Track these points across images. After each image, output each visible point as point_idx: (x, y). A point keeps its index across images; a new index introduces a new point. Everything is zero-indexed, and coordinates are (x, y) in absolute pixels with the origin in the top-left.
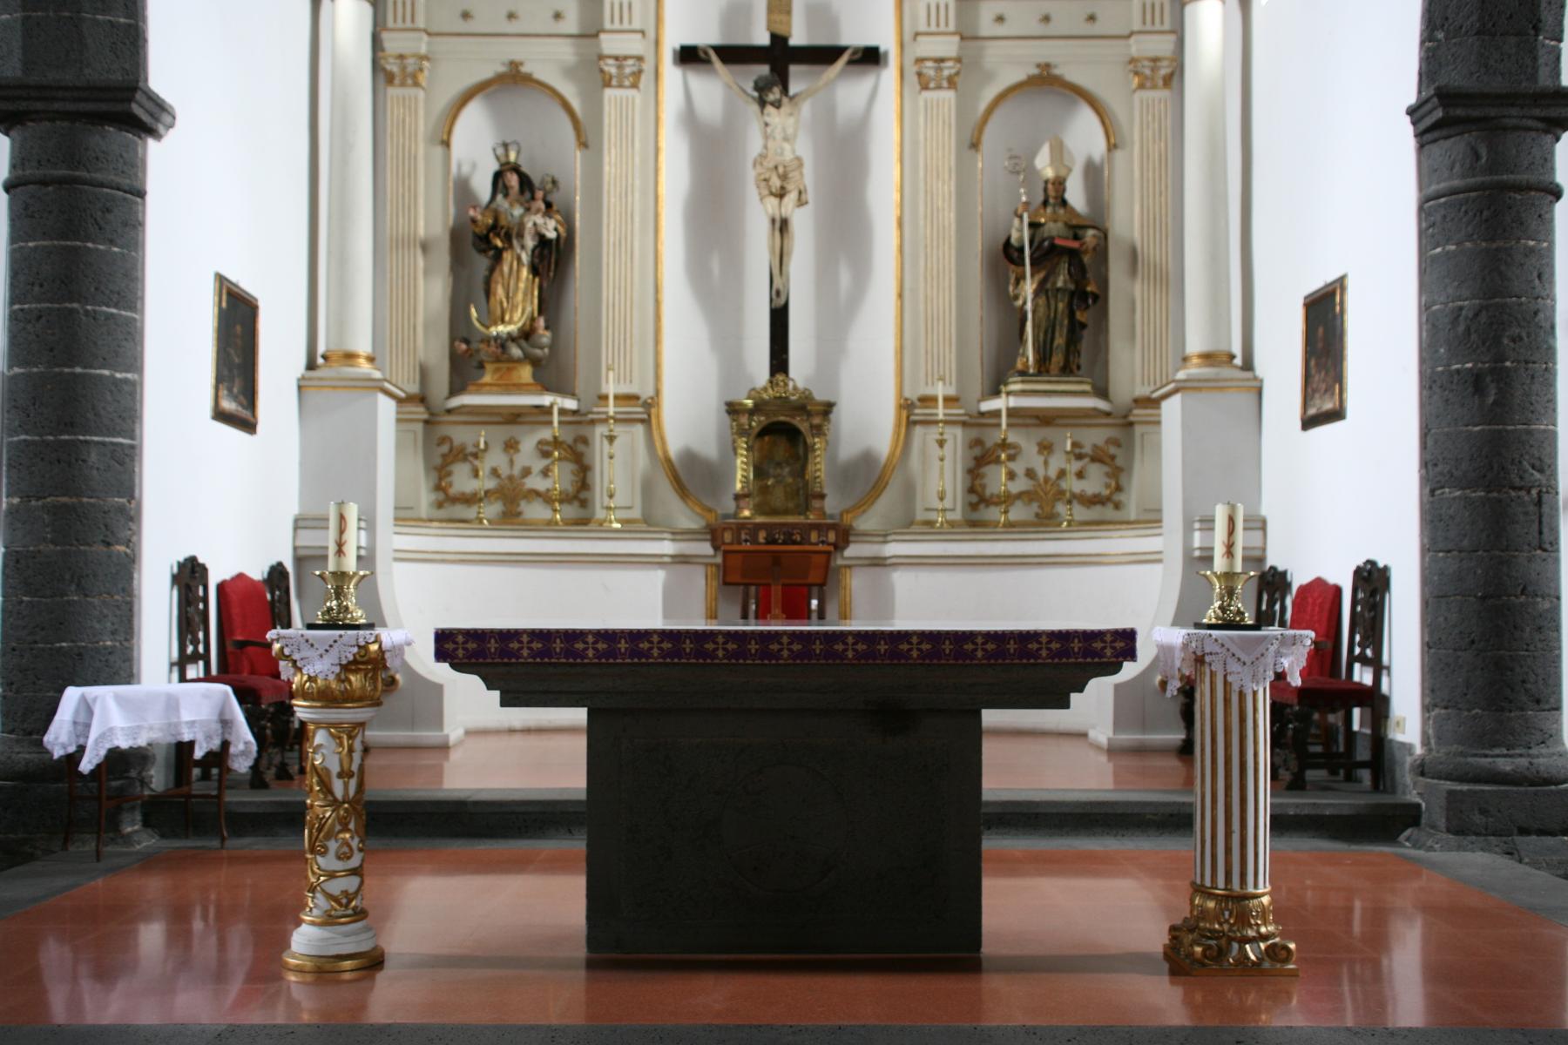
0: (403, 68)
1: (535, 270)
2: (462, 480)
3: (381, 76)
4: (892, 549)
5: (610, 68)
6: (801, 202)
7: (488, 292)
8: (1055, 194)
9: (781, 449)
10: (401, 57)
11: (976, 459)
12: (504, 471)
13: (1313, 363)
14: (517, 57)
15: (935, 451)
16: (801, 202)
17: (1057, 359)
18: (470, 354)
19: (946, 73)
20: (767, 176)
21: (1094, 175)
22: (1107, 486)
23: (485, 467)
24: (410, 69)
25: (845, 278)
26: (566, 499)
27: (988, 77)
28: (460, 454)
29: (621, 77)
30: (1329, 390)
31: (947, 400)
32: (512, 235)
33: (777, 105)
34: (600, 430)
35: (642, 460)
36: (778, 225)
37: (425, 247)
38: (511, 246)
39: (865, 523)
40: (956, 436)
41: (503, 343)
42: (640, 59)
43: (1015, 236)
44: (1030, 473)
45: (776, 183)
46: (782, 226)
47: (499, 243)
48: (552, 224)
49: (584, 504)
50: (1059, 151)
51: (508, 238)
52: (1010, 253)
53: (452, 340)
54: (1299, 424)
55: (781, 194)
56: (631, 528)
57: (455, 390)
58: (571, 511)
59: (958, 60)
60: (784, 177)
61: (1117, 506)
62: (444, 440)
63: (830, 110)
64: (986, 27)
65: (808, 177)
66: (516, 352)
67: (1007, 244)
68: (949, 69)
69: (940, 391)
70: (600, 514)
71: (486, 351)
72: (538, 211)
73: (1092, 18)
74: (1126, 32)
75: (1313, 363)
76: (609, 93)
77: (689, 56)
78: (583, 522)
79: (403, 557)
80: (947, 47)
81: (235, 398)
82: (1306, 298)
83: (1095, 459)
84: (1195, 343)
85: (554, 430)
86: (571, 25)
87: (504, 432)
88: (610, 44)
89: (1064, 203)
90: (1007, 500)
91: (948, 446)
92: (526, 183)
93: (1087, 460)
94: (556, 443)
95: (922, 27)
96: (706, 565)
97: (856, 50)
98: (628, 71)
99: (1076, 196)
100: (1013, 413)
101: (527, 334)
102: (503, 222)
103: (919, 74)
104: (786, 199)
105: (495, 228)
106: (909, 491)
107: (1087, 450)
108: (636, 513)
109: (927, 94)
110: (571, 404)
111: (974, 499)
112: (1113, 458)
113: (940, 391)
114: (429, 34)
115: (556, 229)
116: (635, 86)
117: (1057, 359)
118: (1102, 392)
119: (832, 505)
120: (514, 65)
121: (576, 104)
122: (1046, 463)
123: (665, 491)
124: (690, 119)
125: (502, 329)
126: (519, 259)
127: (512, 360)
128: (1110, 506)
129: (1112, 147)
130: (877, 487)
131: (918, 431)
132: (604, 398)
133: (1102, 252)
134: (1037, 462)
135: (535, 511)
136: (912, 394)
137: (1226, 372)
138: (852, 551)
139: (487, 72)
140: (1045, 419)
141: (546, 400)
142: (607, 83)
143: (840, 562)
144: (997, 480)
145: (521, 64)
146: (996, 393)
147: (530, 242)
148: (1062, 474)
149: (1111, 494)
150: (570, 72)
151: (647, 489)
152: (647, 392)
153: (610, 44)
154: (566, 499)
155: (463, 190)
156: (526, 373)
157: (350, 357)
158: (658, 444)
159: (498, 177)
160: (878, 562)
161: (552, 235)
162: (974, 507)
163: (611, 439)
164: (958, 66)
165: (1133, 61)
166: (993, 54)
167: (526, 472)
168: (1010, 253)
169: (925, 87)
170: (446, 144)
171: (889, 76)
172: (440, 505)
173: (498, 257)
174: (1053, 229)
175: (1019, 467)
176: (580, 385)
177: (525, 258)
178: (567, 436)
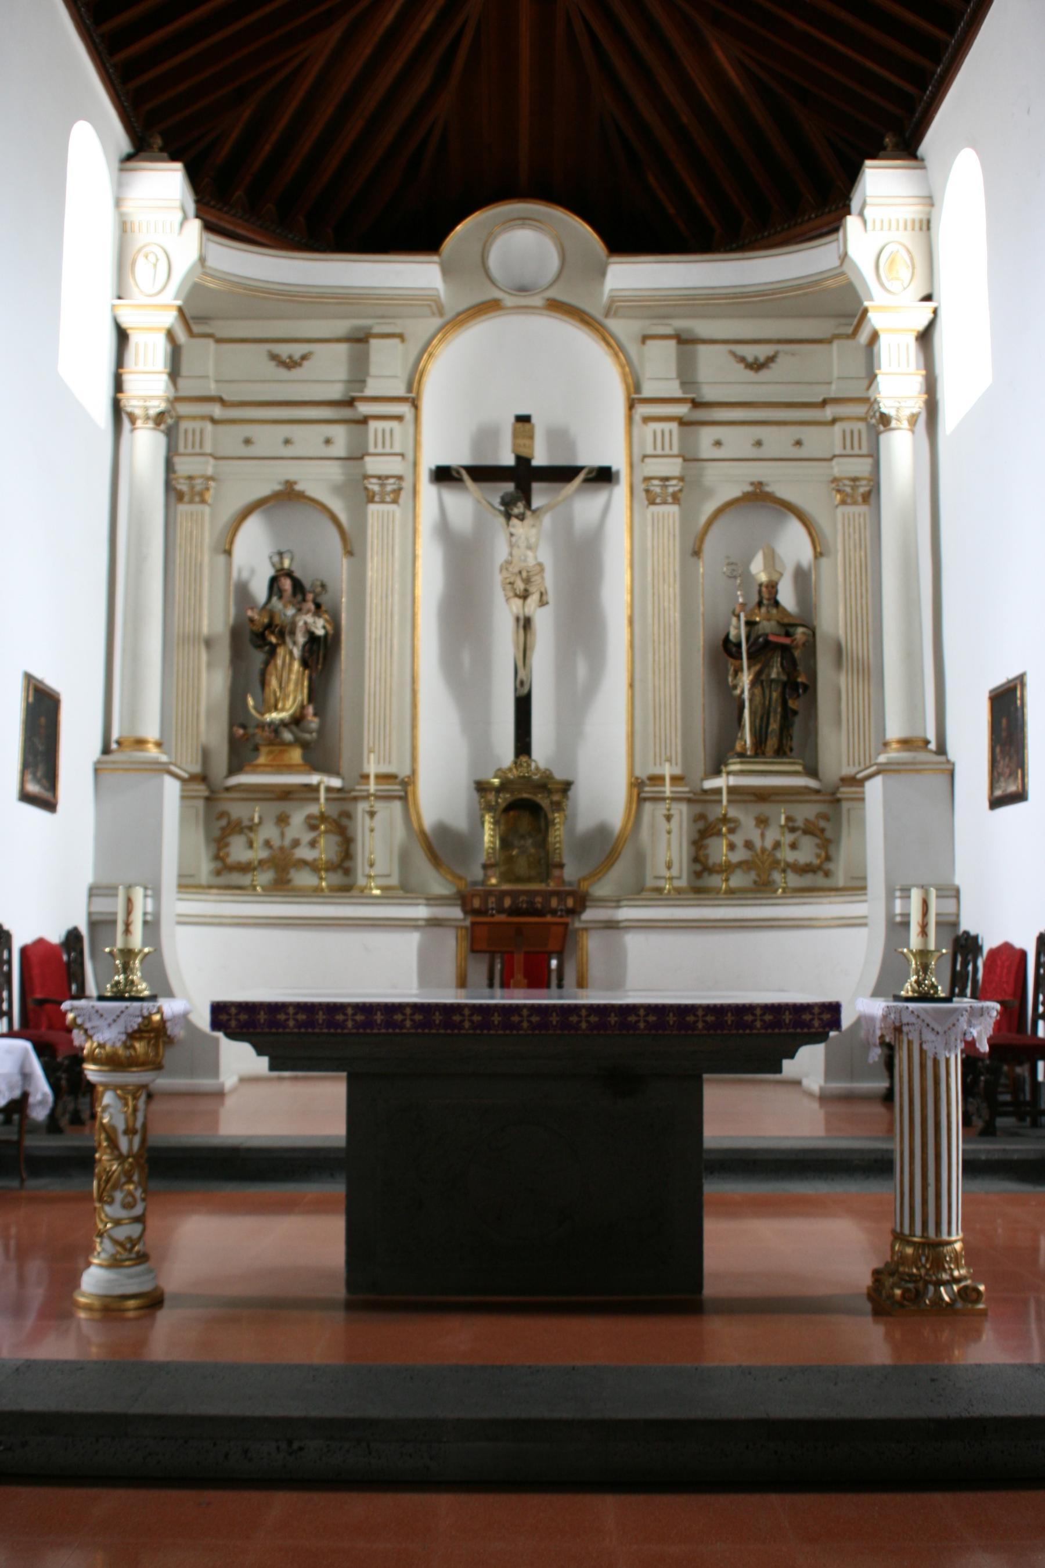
0: (192, 487)
1: (305, 663)
2: (239, 851)
3: (173, 495)
4: (625, 913)
5: (374, 486)
6: (543, 603)
7: (263, 683)
8: (768, 596)
9: (525, 822)
10: (190, 478)
12: (276, 842)
13: (998, 750)
14: (292, 477)
15: (663, 824)
16: (543, 603)
17: (772, 743)
18: (247, 738)
19: (671, 490)
20: (512, 580)
21: (802, 578)
22: (818, 856)
23: (260, 838)
24: (198, 488)
25: (582, 670)
26: (331, 867)
27: (708, 493)
28: (236, 827)
29: (383, 494)
30: (1012, 774)
31: (676, 779)
32: (284, 632)
33: (521, 517)
34: (362, 807)
35: (400, 833)
36: (522, 623)
37: (209, 643)
38: (284, 642)
39: (601, 889)
40: (682, 812)
41: (276, 728)
42: (400, 478)
43: (733, 632)
44: (749, 845)
45: (520, 586)
46: (526, 624)
47: (273, 639)
48: (320, 622)
49: (348, 872)
50: (772, 560)
51: (281, 635)
52: (729, 648)
53: (232, 724)
54: (986, 804)
55: (525, 596)
56: (389, 895)
57: (233, 771)
58: (336, 878)
59: (681, 479)
60: (527, 581)
61: (827, 874)
62: (223, 814)
63: (567, 525)
64: (706, 450)
65: (549, 581)
66: (288, 736)
67: (727, 640)
68: (673, 486)
69: (668, 770)
70: (361, 881)
71: (261, 736)
72: (308, 612)
73: (799, 443)
74: (828, 456)
75: (998, 750)
76: (372, 508)
77: (443, 475)
79: (185, 921)
80: (672, 467)
81: (38, 781)
82: (991, 692)
83: (806, 832)
84: (894, 731)
85: (321, 805)
86: (339, 448)
87: (277, 807)
88: (374, 465)
89: (776, 604)
90: (728, 869)
91: (675, 821)
92: (298, 587)
93: (799, 833)
94: (323, 817)
95: (650, 451)
96: (457, 927)
97: (592, 470)
98: (389, 488)
99: (787, 597)
100: (732, 790)
101: (297, 721)
102: (277, 621)
103: (647, 491)
104: (529, 601)
105: (270, 626)
106: (640, 860)
107: (800, 823)
108: (394, 881)
109: (653, 508)
110: (336, 782)
111: (698, 867)
112: (823, 830)
113: (668, 770)
114: (216, 458)
115: (324, 627)
116: (395, 501)
117: (772, 743)
118: (812, 771)
119: (570, 873)
120: (290, 484)
121: (343, 517)
122: (763, 835)
123: (421, 860)
124: (444, 530)
125: (275, 716)
126: (291, 653)
127: (284, 744)
128: (820, 874)
129: (818, 555)
130: (611, 857)
131: (648, 806)
132: (366, 777)
133: (810, 647)
134: (755, 835)
135: (304, 878)
136: (641, 773)
137: (922, 756)
138: (589, 915)
139: (264, 490)
140: (761, 796)
142: (371, 499)
143: (577, 925)
144: (719, 850)
145: (295, 483)
146: (717, 772)
147: (301, 639)
148: (777, 845)
149: (822, 863)
150: (338, 490)
151: (404, 859)
152: (404, 772)
153: (374, 465)
154: (331, 867)
155: (242, 593)
156: (296, 755)
157: (140, 743)
158: (414, 818)
159: (274, 581)
160: (612, 925)
161: (320, 632)
162: (698, 875)
163: (372, 814)
164: (681, 484)
165: (835, 480)
166: (712, 474)
167: (296, 843)
168: (729, 648)
169: (652, 502)
170: (229, 553)
171: (620, 492)
172: (218, 873)
173: (272, 652)
174: (767, 627)
175: (738, 839)
176: (345, 765)
177: (297, 652)
178: (333, 811)
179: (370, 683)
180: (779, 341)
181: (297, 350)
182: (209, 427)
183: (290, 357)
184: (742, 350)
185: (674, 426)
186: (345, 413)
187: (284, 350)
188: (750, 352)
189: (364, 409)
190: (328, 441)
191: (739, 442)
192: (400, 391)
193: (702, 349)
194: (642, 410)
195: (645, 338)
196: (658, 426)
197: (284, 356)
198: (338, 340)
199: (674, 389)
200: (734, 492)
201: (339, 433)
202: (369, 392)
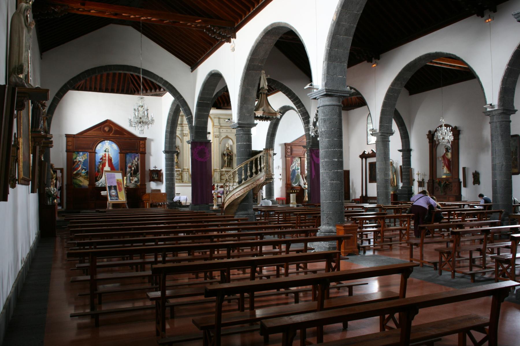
27: (221, 136)
34: (185, 173)
43: (224, 153)
64: (221, 131)
67: (223, 154)
78: (182, 182)
80: (218, 134)
99: (230, 149)
100: (225, 171)
121: (180, 138)
129: (233, 144)
133: (233, 155)
141: (179, 169)
142: (184, 136)
144: (223, 177)
150: (180, 134)
162: (220, 180)
166: (222, 134)
174: (228, 152)
176: (181, 168)
179: (185, 158)
189: (183, 125)
191: (225, 130)
193: (221, 119)
194: (214, 127)
200: (224, 136)
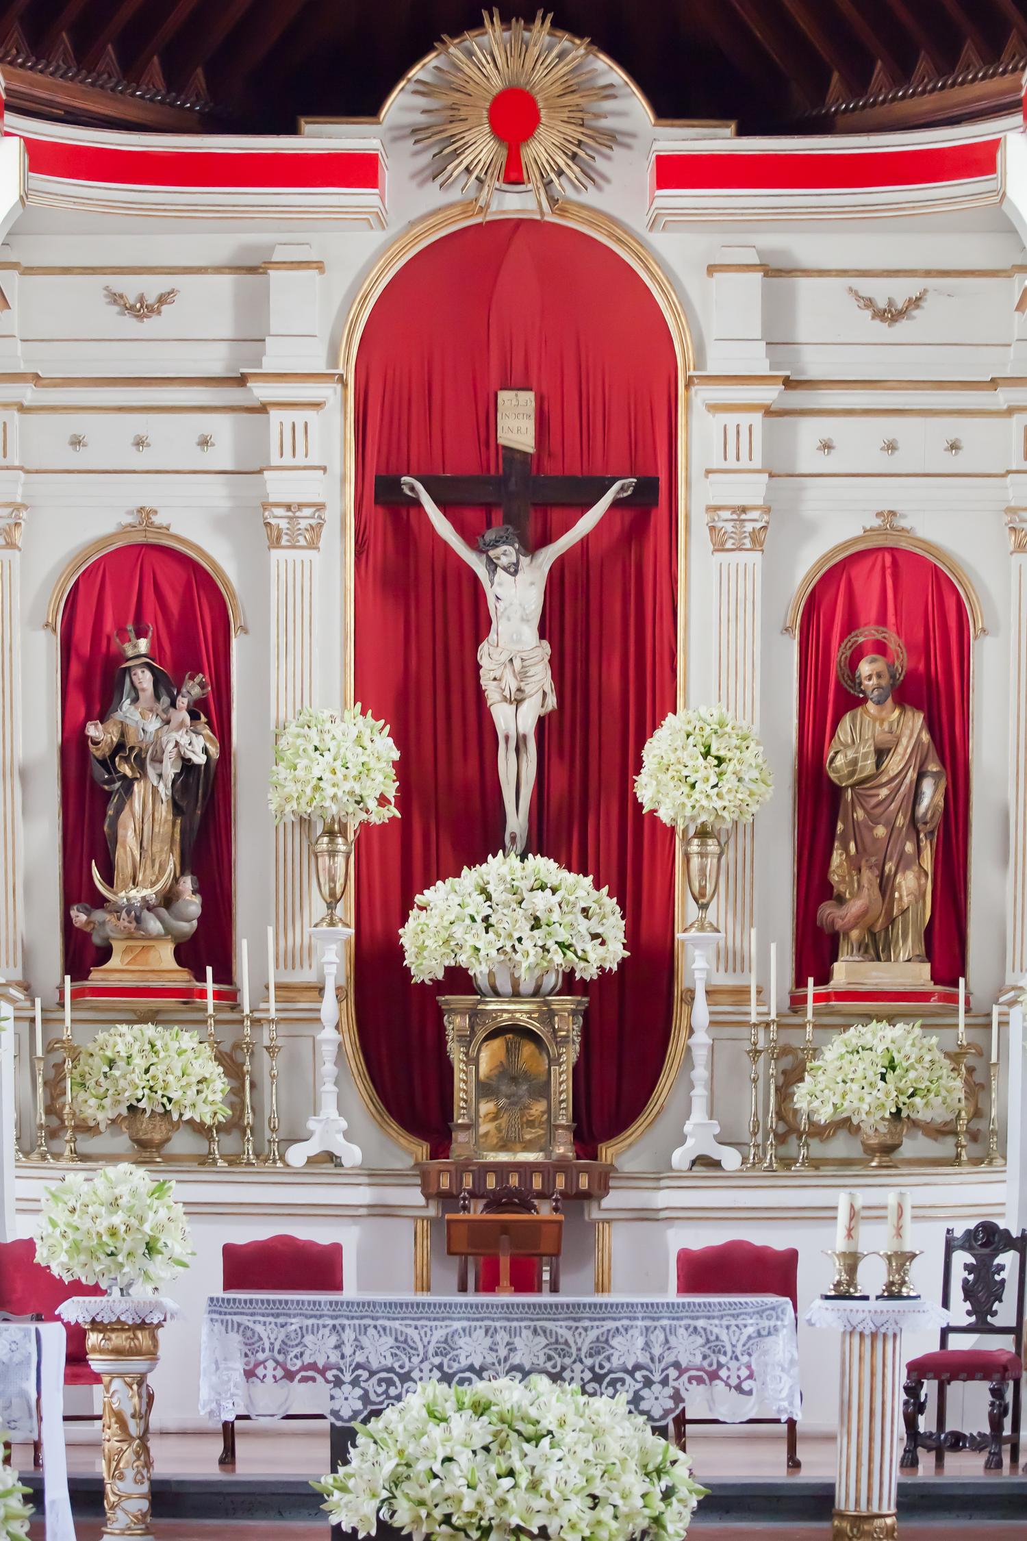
11: (784, 1072)
14: (149, 504)
19: (749, 527)
20: (497, 674)
27: (809, 530)
29: (293, 533)
37: (24, 776)
38: (144, 774)
42: (320, 507)
47: (126, 770)
48: (199, 742)
59: (767, 510)
64: (808, 459)
66: (154, 925)
68: (752, 524)
72: (181, 725)
73: (954, 446)
74: (1003, 472)
76: (276, 554)
80: (752, 490)
88: (279, 486)
95: (717, 463)
96: (415, 1218)
98: (304, 524)
102: (131, 741)
103: (712, 529)
104: (524, 707)
115: (205, 750)
116: (313, 545)
125: (136, 894)
126: (155, 790)
127: (149, 937)
138: (612, 1200)
142: (275, 542)
143: (596, 1215)
147: (170, 769)
150: (222, 524)
160: (646, 1216)
161: (200, 759)
164: (766, 518)
166: (816, 497)
169: (720, 548)
177: (164, 791)
180: (928, 273)
181: (152, 287)
182: (16, 415)
183: (141, 299)
184: (867, 286)
185: (757, 418)
186: (233, 396)
187: (131, 287)
188: (883, 291)
189: (261, 392)
190: (204, 442)
192: (321, 367)
193: (803, 283)
195: (712, 269)
196: (732, 419)
197: (131, 299)
198: (218, 270)
199: (757, 360)
201: (222, 427)
202: (268, 366)
